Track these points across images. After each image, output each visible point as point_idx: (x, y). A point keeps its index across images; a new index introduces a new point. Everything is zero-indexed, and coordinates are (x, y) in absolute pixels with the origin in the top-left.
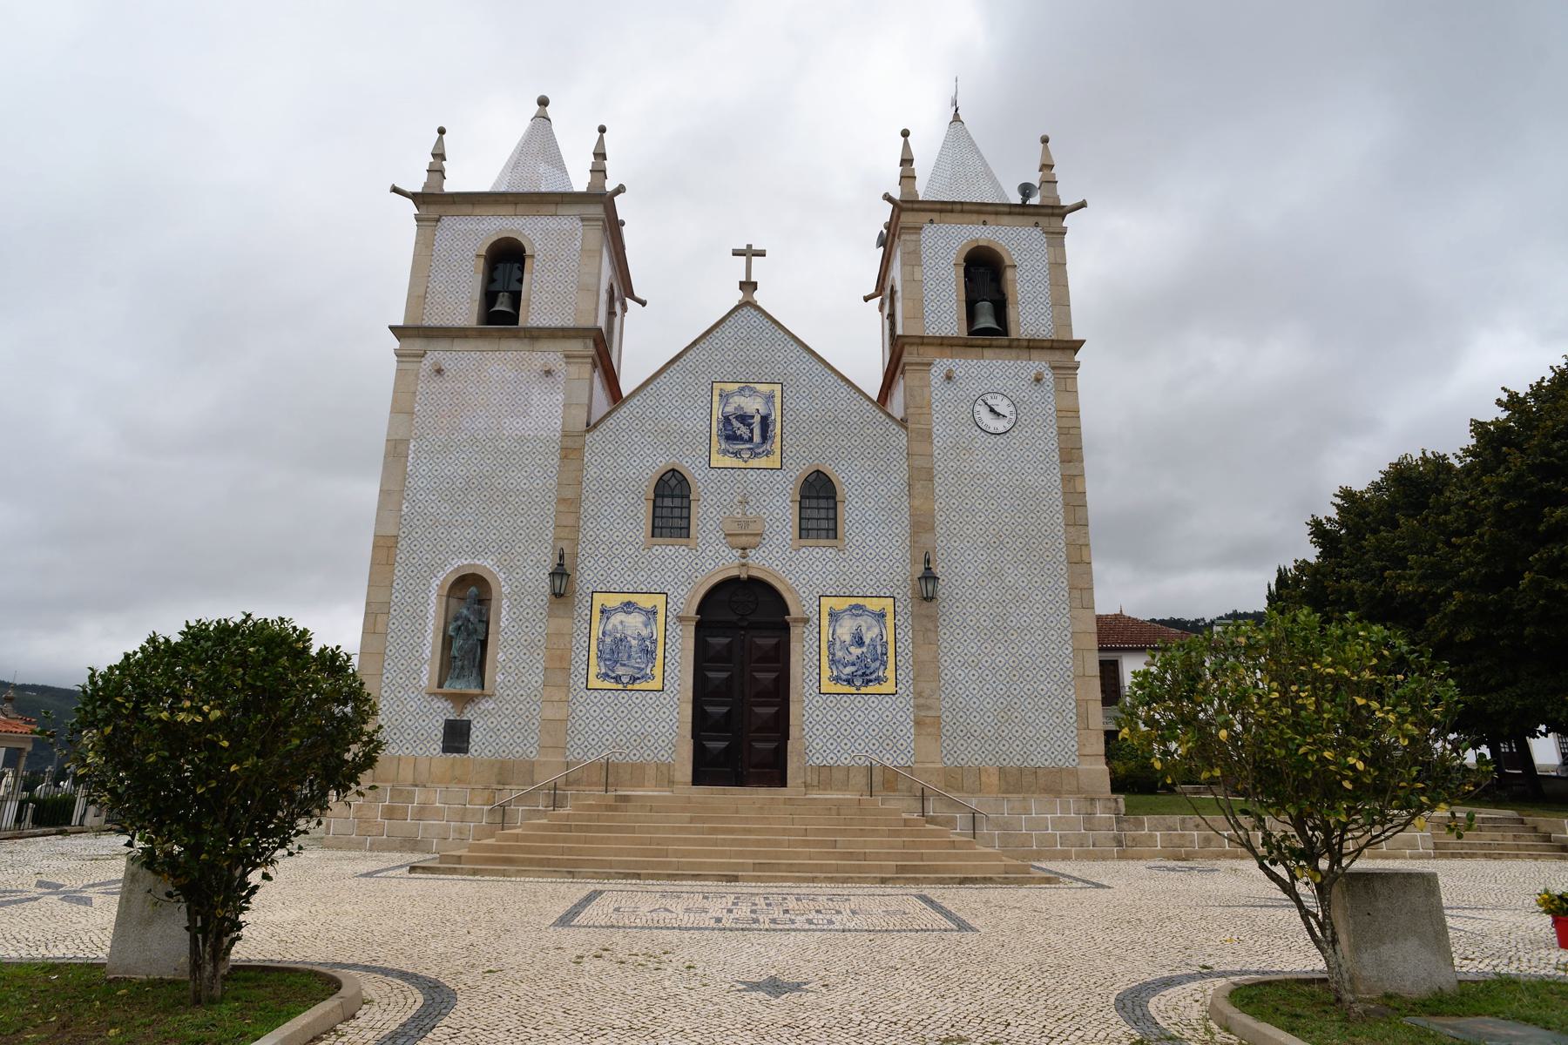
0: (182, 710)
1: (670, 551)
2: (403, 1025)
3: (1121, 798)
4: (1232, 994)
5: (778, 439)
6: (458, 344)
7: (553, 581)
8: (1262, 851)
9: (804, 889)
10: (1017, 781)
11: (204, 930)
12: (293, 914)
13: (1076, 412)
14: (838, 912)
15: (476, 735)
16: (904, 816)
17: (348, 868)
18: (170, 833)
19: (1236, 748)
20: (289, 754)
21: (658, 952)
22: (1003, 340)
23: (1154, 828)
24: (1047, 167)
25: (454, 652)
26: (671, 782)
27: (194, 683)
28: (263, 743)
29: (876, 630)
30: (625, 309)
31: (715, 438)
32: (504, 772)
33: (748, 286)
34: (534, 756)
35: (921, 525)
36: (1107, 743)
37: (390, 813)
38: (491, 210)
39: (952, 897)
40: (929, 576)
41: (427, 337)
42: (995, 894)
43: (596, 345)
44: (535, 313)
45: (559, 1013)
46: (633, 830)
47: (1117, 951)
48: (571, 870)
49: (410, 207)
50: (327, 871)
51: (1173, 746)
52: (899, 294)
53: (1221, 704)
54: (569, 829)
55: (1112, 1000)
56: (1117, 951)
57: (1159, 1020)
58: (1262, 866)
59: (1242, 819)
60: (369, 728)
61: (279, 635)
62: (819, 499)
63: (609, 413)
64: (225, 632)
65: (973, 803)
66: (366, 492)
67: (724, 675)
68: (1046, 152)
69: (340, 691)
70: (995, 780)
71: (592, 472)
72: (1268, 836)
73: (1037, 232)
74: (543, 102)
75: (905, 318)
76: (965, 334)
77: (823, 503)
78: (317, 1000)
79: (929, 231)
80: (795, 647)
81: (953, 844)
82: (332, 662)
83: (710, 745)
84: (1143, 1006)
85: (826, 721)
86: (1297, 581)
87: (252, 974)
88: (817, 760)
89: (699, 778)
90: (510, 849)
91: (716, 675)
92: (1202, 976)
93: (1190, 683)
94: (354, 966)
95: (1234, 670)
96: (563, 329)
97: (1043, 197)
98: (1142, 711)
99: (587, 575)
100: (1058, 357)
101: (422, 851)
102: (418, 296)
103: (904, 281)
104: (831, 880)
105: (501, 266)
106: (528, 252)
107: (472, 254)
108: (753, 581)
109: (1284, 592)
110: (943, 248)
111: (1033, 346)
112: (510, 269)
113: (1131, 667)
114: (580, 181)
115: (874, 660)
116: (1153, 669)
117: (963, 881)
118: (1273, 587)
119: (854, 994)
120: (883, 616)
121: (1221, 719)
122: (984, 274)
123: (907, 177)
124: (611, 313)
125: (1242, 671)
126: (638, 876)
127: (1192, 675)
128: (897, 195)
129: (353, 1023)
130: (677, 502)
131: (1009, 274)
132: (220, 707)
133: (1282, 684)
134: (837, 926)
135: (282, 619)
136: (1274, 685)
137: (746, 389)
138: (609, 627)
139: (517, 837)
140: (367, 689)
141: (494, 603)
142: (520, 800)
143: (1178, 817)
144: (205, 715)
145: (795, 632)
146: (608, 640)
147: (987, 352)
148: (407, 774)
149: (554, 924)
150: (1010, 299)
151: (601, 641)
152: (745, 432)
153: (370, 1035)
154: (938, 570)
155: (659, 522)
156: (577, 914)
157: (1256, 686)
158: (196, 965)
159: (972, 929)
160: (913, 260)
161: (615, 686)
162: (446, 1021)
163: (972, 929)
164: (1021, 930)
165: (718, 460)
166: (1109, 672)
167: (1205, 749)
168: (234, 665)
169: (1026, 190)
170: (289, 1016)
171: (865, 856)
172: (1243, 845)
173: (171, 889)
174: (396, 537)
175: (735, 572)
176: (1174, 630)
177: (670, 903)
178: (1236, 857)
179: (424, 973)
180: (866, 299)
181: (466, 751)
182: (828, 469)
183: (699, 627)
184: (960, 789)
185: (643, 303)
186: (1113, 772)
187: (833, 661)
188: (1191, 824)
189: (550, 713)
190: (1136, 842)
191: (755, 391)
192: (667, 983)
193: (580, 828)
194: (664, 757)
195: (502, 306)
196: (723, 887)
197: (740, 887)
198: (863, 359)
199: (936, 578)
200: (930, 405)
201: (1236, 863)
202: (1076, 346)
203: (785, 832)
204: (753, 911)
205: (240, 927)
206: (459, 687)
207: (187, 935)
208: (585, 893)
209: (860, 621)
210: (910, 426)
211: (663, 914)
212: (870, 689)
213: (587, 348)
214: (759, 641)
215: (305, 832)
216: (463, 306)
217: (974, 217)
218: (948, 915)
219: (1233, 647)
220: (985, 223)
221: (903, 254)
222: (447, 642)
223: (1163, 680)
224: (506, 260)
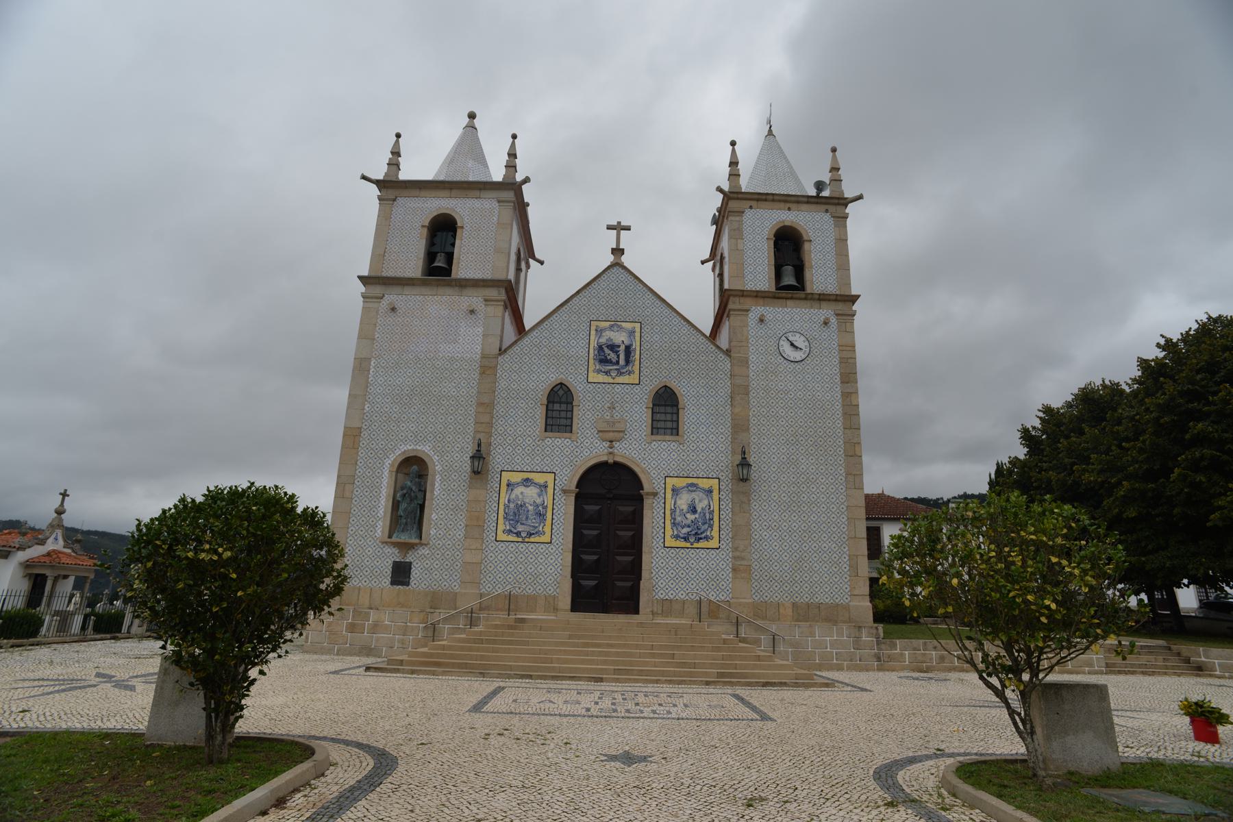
0: (203, 551)
1: (558, 442)
2: (359, 782)
3: (880, 627)
4: (957, 770)
5: (637, 363)
6: (407, 290)
7: (473, 463)
8: (981, 666)
9: (650, 688)
10: (806, 613)
11: (216, 710)
12: (281, 700)
13: (853, 347)
14: (675, 706)
15: (415, 573)
17: (321, 667)
18: (193, 639)
19: (964, 592)
20: (280, 585)
22: (801, 294)
23: (904, 649)
24: (835, 169)
25: (401, 512)
26: (556, 610)
27: (212, 531)
28: (261, 576)
29: (706, 502)
30: (528, 266)
31: (591, 361)
32: (435, 600)
33: (618, 251)
34: (457, 589)
35: (740, 427)
36: (871, 586)
37: (352, 628)
39: (758, 697)
40: (744, 464)
41: (384, 284)
42: (787, 694)
44: (464, 267)
45: (472, 775)
46: (527, 643)
47: (876, 737)
48: (482, 672)
49: (374, 190)
50: (306, 669)
51: (919, 589)
52: (726, 260)
54: (482, 642)
56: (876, 737)
57: (905, 787)
58: (981, 678)
59: (967, 643)
60: (338, 566)
61: (274, 497)
62: (666, 406)
63: (516, 342)
64: (235, 495)
65: (774, 628)
66: (339, 395)
67: (595, 532)
68: (834, 159)
70: (789, 612)
71: (502, 384)
72: (985, 655)
73: (827, 217)
74: (472, 116)
75: (730, 277)
76: (773, 289)
77: (669, 409)
78: (297, 763)
79: (749, 214)
80: (647, 513)
81: (758, 658)
82: (312, 518)
84: (893, 777)
85: (667, 568)
86: (1010, 472)
87: (250, 743)
88: (661, 595)
89: (576, 607)
90: (438, 656)
92: (936, 756)
94: (325, 738)
95: (963, 536)
96: (483, 280)
97: (832, 191)
98: (896, 564)
99: (497, 458)
100: (840, 307)
101: (375, 656)
102: (379, 254)
103: (730, 250)
104: (670, 682)
108: (617, 465)
109: (1001, 480)
110: (759, 227)
111: (822, 298)
112: (446, 236)
113: (889, 532)
114: (498, 175)
115: (704, 524)
116: (905, 534)
117: (765, 685)
118: (993, 476)
119: (685, 765)
120: (710, 491)
121: (953, 571)
122: (788, 245)
123: (734, 175)
124: (518, 270)
125: (969, 536)
126: (530, 677)
128: (726, 188)
129: (323, 779)
130: (564, 407)
131: (806, 246)
132: (231, 549)
133: (998, 546)
134: (674, 715)
135: (276, 487)
136: (993, 547)
138: (513, 496)
140: (337, 538)
141: (430, 477)
144: (220, 555)
145: (647, 502)
146: (512, 505)
147: (789, 302)
149: (469, 711)
150: (807, 264)
151: (506, 506)
152: (611, 357)
153: (335, 788)
154: (751, 460)
155: (550, 421)
156: (486, 703)
157: (979, 547)
158: (210, 736)
160: (737, 234)
164: (806, 721)
165: (594, 377)
166: (874, 536)
167: (942, 592)
168: (242, 519)
169: (820, 186)
170: (276, 774)
171: (695, 666)
172: (967, 662)
175: (604, 458)
176: (920, 506)
177: (554, 697)
178: (962, 670)
179: (375, 744)
180: (703, 263)
181: (408, 584)
182: (673, 385)
184: (764, 618)
185: (542, 263)
186: (875, 607)
187: (674, 524)
188: (930, 646)
190: (891, 658)
191: (621, 328)
192: (550, 755)
193: (488, 642)
194: (551, 591)
195: (440, 262)
196: (592, 686)
197: (604, 686)
200: (747, 340)
201: (963, 675)
202: (853, 299)
203: (637, 647)
204: (613, 704)
205: (242, 709)
206: (404, 538)
207: (204, 714)
208: (492, 688)
209: (694, 495)
211: (548, 705)
212: (702, 544)
214: (621, 508)
215: (291, 641)
216: (411, 262)
217: (782, 205)
218: (754, 708)
219: (963, 518)
220: (789, 209)
221: (730, 231)
222: (396, 505)
223: (912, 542)
224: (443, 230)
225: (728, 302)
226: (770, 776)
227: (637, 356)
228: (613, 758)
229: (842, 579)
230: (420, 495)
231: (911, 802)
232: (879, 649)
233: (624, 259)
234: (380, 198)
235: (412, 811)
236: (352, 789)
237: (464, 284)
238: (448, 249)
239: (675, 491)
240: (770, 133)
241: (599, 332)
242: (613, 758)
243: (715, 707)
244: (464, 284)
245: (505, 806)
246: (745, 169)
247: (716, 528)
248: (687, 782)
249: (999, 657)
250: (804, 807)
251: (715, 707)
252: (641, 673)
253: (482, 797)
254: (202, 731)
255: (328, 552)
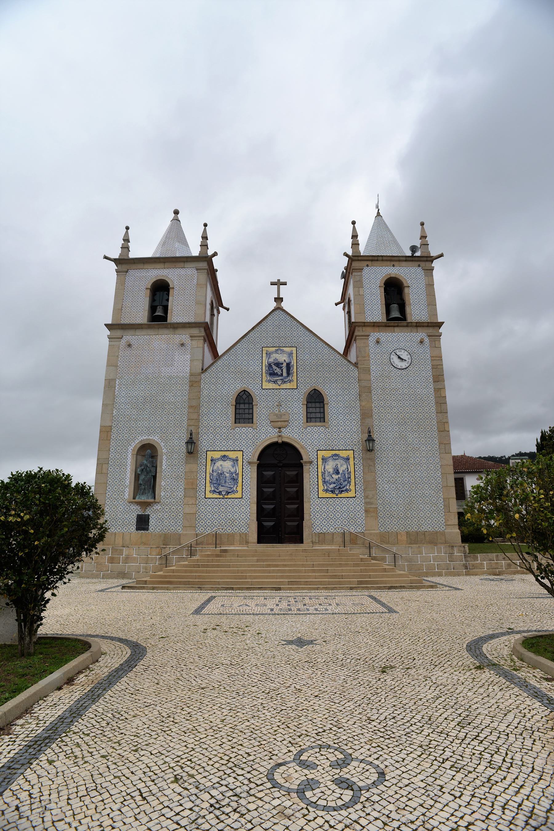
0: (11, 515)
1: (244, 430)
2: (121, 665)
3: (467, 546)
4: (524, 642)
5: (295, 374)
6: (138, 332)
7: (187, 446)
8: (537, 573)
9: (313, 593)
10: (416, 538)
11: (24, 621)
12: (67, 611)
14: (330, 605)
15: (152, 522)
16: (361, 556)
17: (93, 587)
18: (7, 575)
19: (522, 520)
20: (63, 536)
21: (243, 626)
22: (404, 323)
23: (483, 560)
24: (423, 237)
25: (140, 482)
26: (247, 543)
27: (16, 502)
28: (50, 531)
29: (345, 466)
30: (219, 312)
31: (264, 375)
32: (166, 539)
33: (279, 300)
35: (366, 414)
36: (459, 518)
37: (112, 560)
39: (385, 596)
40: (370, 439)
41: (122, 329)
42: (406, 594)
43: (205, 330)
46: (229, 566)
47: (467, 622)
48: (200, 587)
50: (82, 589)
51: (492, 522)
52: (352, 302)
53: (515, 501)
55: (465, 646)
56: (467, 622)
58: (537, 580)
59: (526, 556)
60: (101, 521)
61: (56, 478)
62: (315, 402)
63: (212, 364)
64: (30, 477)
65: (394, 549)
66: (96, 405)
68: (423, 230)
69: (86, 504)
70: (404, 538)
71: (205, 392)
72: (540, 565)
73: (419, 270)
74: (176, 212)
75: (355, 313)
76: (385, 321)
77: (318, 405)
79: (366, 270)
80: (306, 475)
81: (385, 570)
82: (82, 490)
83: (265, 524)
84: (480, 649)
85: (321, 511)
86: (551, 437)
87: (48, 641)
89: (260, 540)
90: (170, 577)
91: (269, 507)
92: (509, 633)
93: (498, 490)
94: (97, 636)
95: (522, 484)
96: (189, 323)
97: (422, 252)
98: (477, 505)
99: (204, 442)
100: (431, 331)
101: (128, 578)
102: (118, 309)
103: (355, 295)
104: (326, 589)
105: (158, 293)
107: (143, 288)
109: (544, 443)
110: (374, 278)
111: (419, 325)
112: (163, 293)
113: (471, 482)
114: (195, 251)
115: (344, 481)
116: (482, 485)
117: (390, 588)
118: (539, 441)
119: (339, 645)
120: (348, 459)
121: (515, 509)
122: (394, 290)
123: (355, 245)
124: (212, 315)
126: (232, 589)
127: (500, 487)
128: (350, 253)
129: (97, 664)
131: (406, 290)
132: (29, 514)
133: (545, 491)
134: (330, 611)
135: (57, 470)
136: (542, 491)
138: (215, 468)
139: (173, 571)
140: (99, 503)
142: (174, 552)
143: (494, 555)
144: (22, 518)
145: (305, 468)
146: (215, 474)
147: (396, 329)
148: (119, 541)
149: (193, 613)
150: (407, 303)
151: (211, 475)
152: (278, 371)
153: (106, 670)
154: (375, 436)
155: (238, 416)
156: (204, 608)
157: (532, 492)
158: (21, 638)
159: (395, 612)
160: (359, 285)
161: (219, 496)
162: (142, 662)
163: (395, 612)
164: (419, 612)
165: (266, 385)
166: (459, 484)
167: (509, 524)
168: (35, 493)
169: (414, 249)
170: (67, 662)
171: (342, 577)
172: (527, 569)
173: (8, 601)
174: (111, 426)
175: (275, 440)
177: (248, 602)
178: (523, 573)
179: (131, 639)
180: (336, 304)
181: (147, 529)
182: (320, 388)
183: (259, 467)
184: (388, 543)
185: (228, 309)
186: (462, 532)
187: (324, 482)
188: (501, 558)
189: (187, 510)
190: (474, 567)
192: (248, 642)
194: (244, 530)
195: (159, 313)
196: (274, 593)
197: (282, 593)
198: (337, 337)
199: (374, 440)
201: (523, 576)
202: (440, 325)
203: (303, 565)
204: (289, 605)
205: (42, 619)
206: (144, 499)
207: (17, 623)
208: (207, 598)
209: (337, 462)
210: (359, 366)
211: (245, 607)
212: (344, 495)
214: (288, 473)
215: (72, 572)
216: (140, 312)
217: (389, 263)
218: (383, 605)
219: (521, 473)
220: (394, 266)
221: (354, 282)
222: (137, 477)
223: (487, 490)
224: (160, 291)
225: (354, 330)
226: (396, 651)
227: (295, 370)
228: (290, 642)
229: (438, 514)
230: (153, 469)
231: (493, 665)
232: (466, 561)
233: (283, 304)
234: (117, 271)
235: (158, 684)
236: (117, 670)
237: (177, 326)
238: (164, 303)
239: (324, 460)
240: (378, 213)
241: (269, 354)
242: (290, 642)
243: (357, 605)
244: (177, 326)
245: (219, 678)
246: (362, 240)
247: (353, 483)
248: (341, 657)
249: (548, 565)
250: (420, 672)
251: (357, 605)
252: (306, 583)
253: (204, 673)
254: (16, 635)
255: (94, 512)
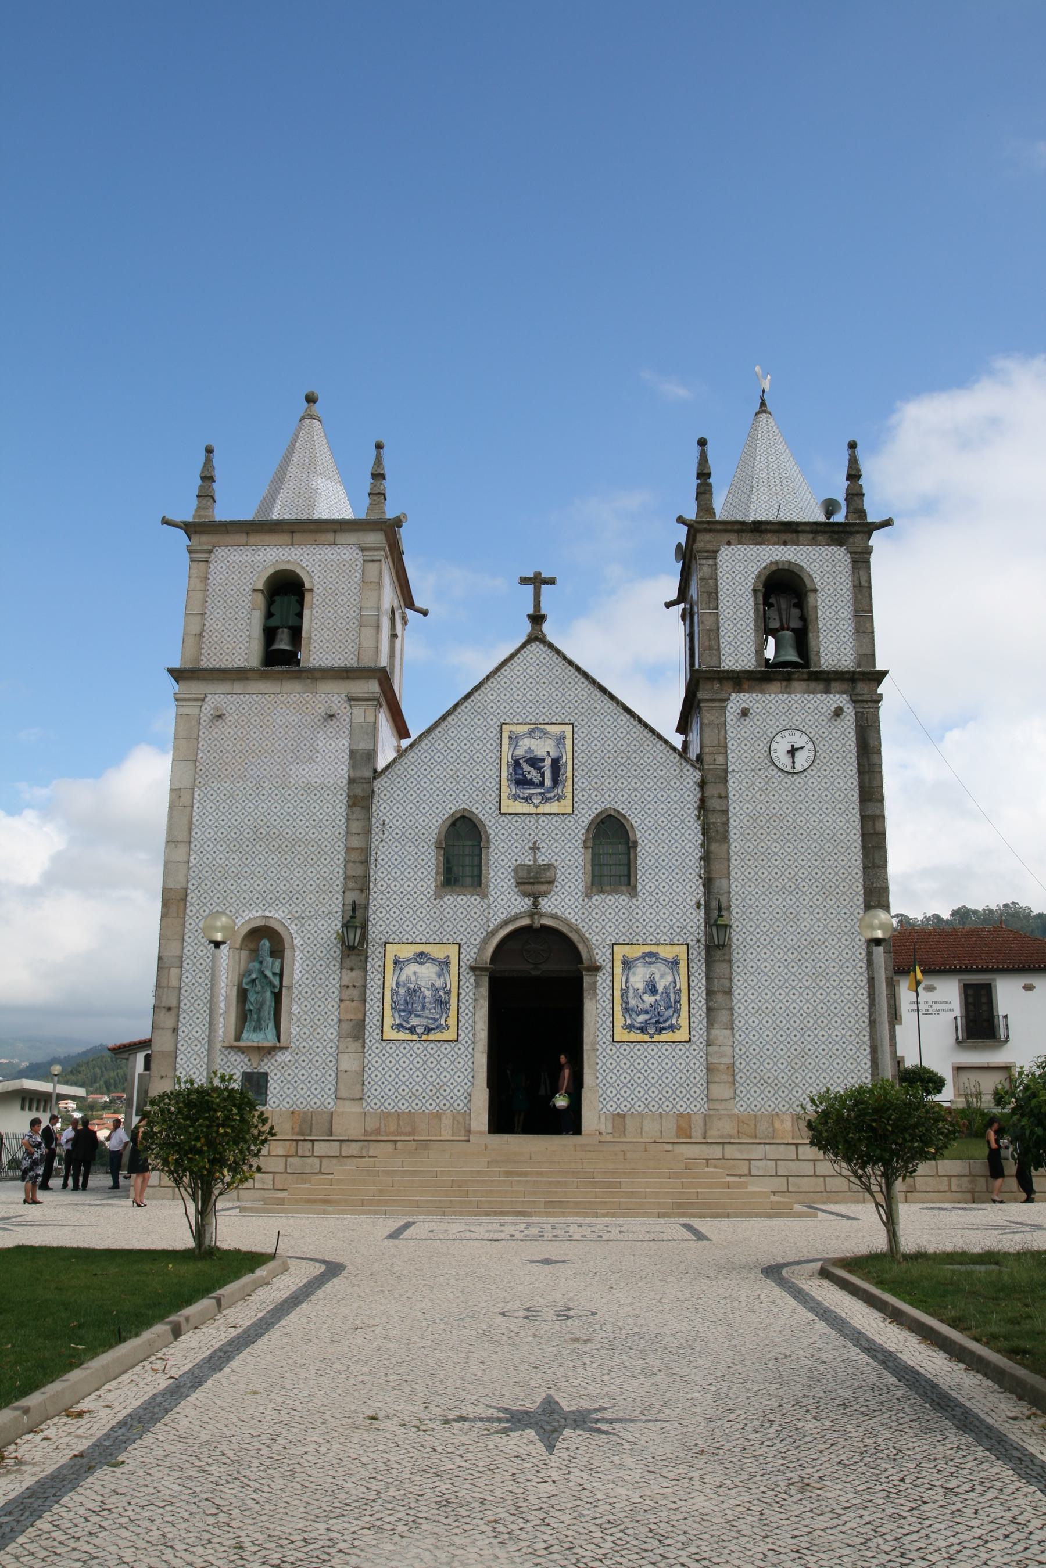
5: (569, 782)
31: (505, 783)
38: (268, 538)
62: (612, 846)
105: (277, 598)
106: (307, 586)
107: (248, 588)
122: (783, 595)
137: (536, 730)
138: (403, 978)
146: (402, 991)
151: (395, 993)
161: (409, 1037)
191: (544, 733)
195: (283, 644)
202: (880, 676)
213: (374, 687)
224: (285, 592)
